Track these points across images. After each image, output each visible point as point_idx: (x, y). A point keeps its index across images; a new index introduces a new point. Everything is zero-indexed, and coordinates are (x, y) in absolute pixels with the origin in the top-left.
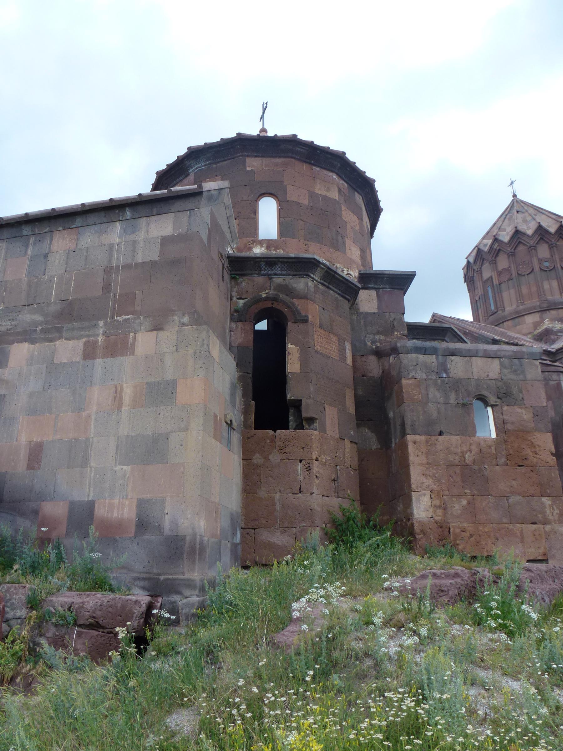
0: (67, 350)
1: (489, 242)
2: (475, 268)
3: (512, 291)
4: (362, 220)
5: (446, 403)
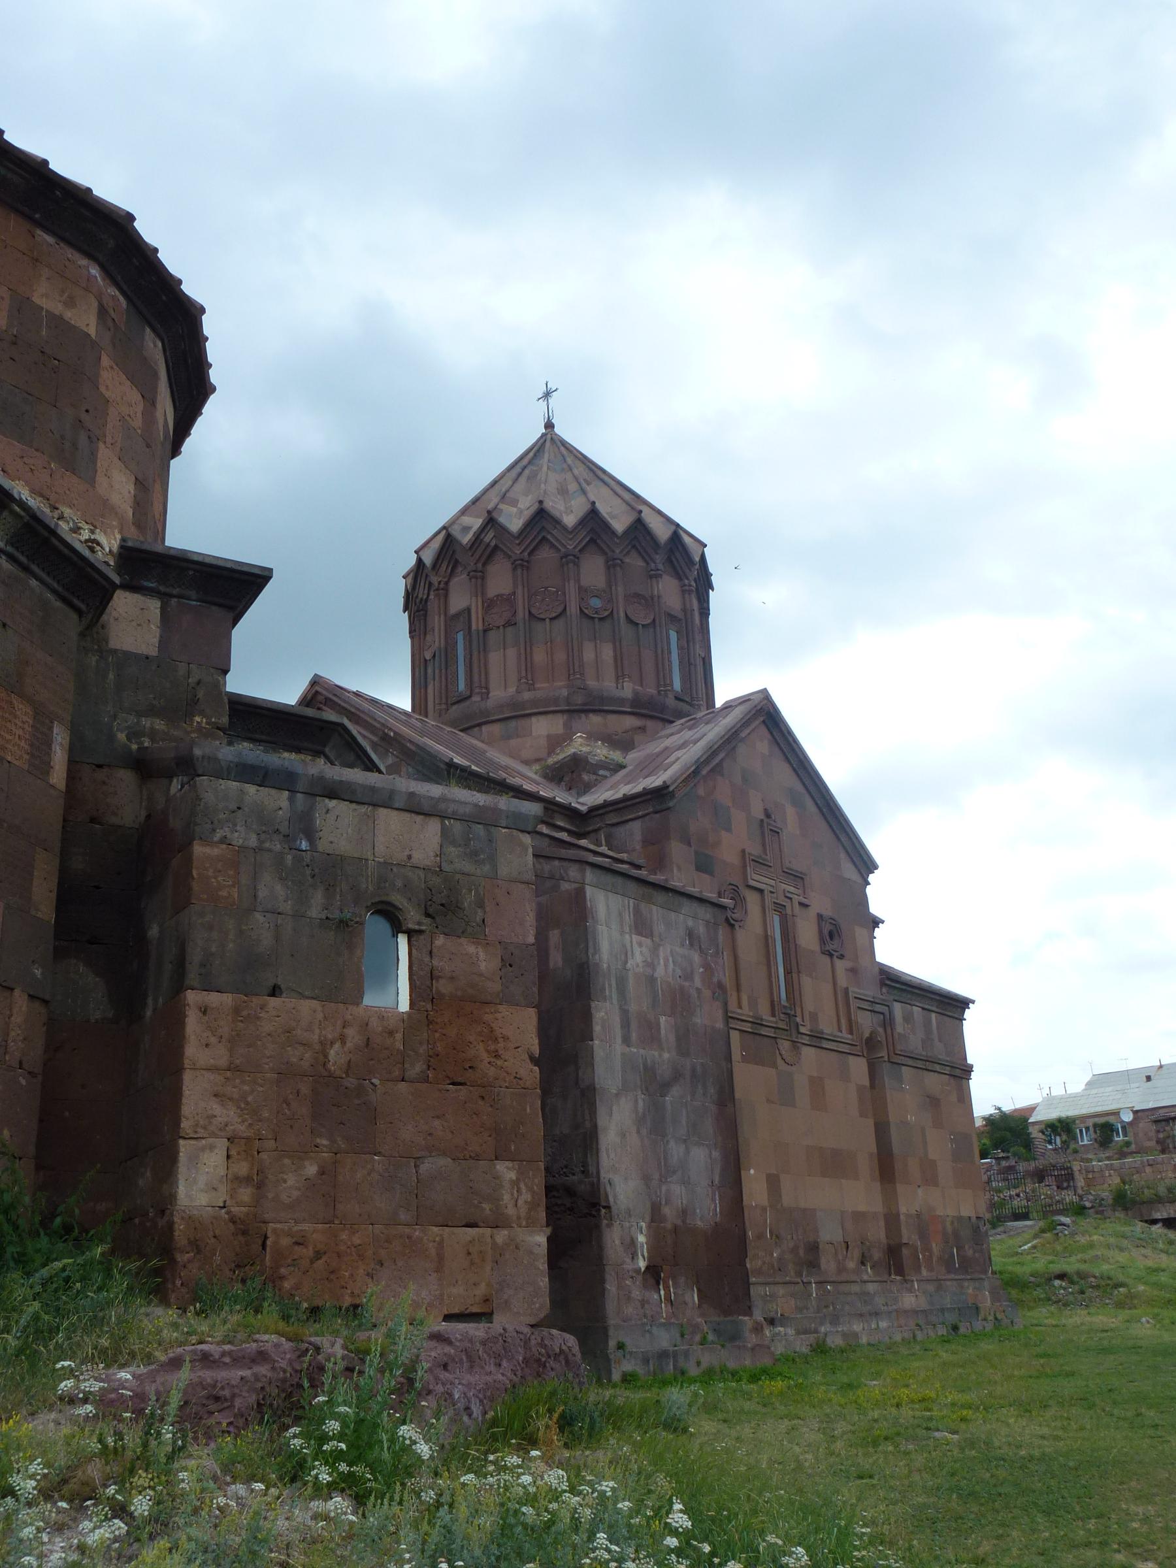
1: (476, 523)
2: (435, 580)
3: (511, 653)
4: (153, 404)
5: (298, 916)
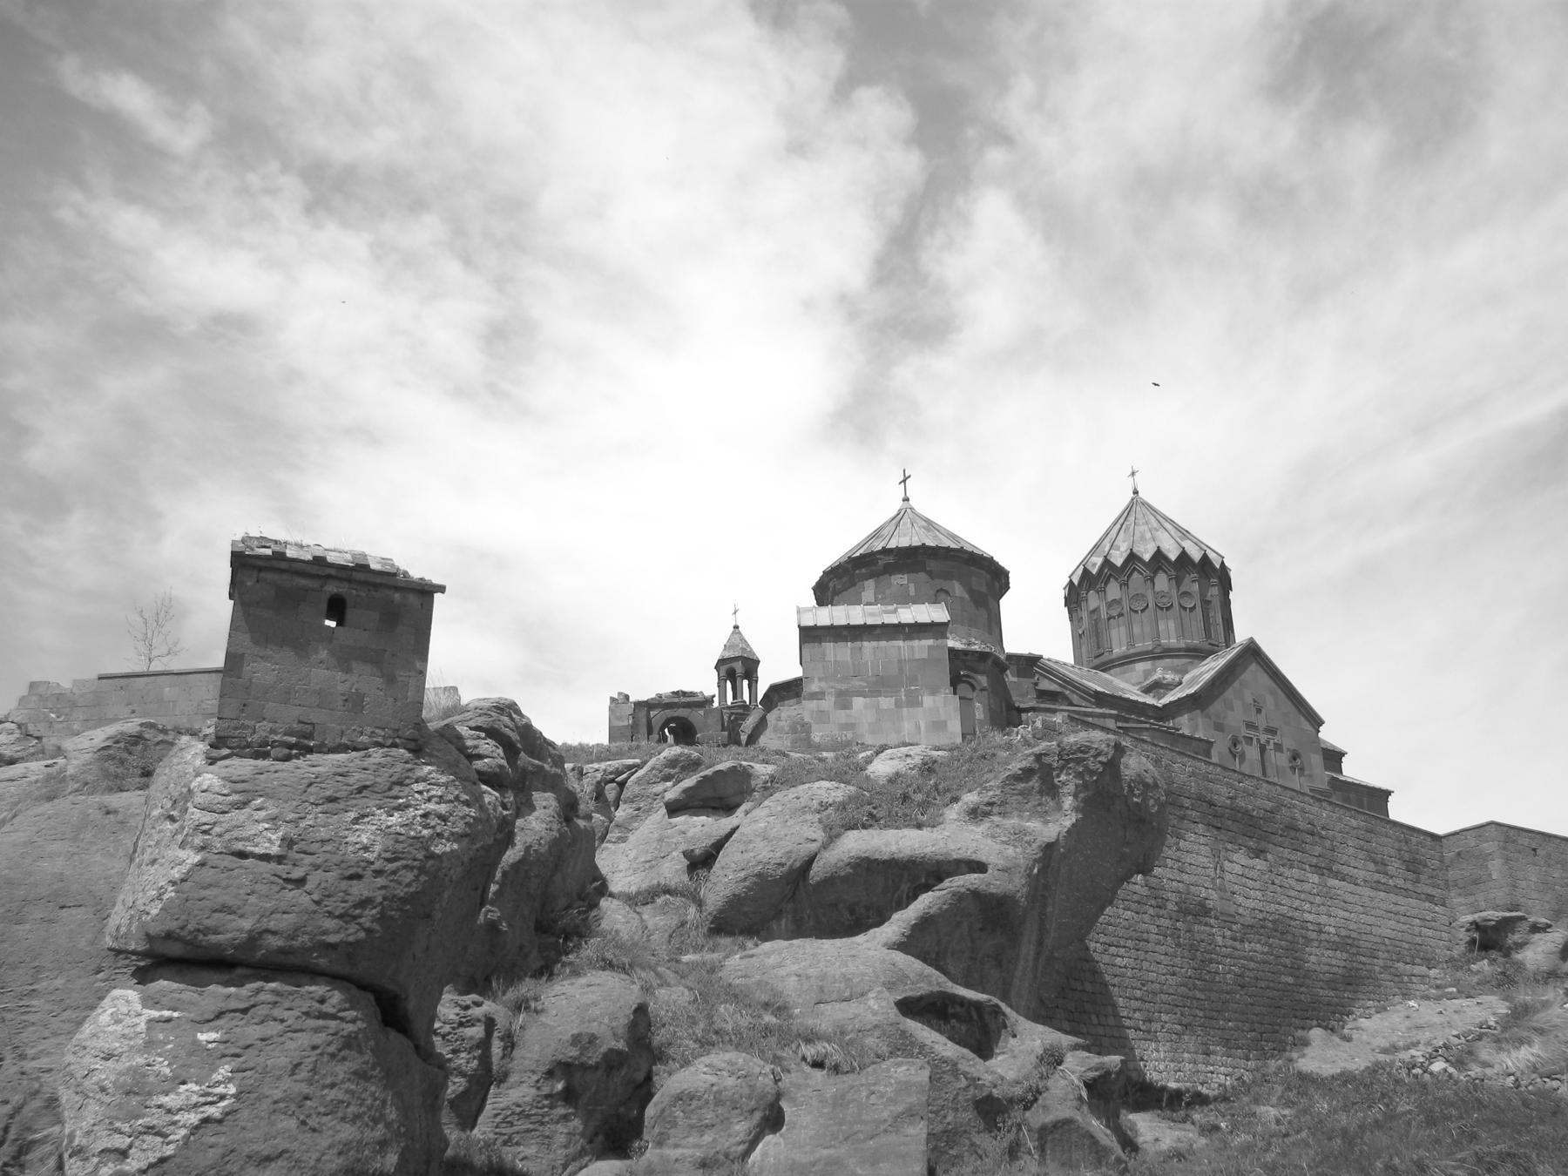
0: (886, 702)
1: (1099, 561)
3: (1123, 629)
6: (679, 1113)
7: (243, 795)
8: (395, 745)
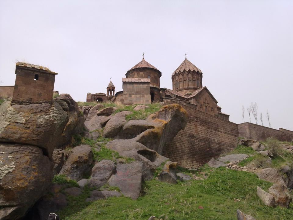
0: (138, 96)
1: (179, 71)
3: (182, 84)
6: (97, 171)
7: (18, 111)
8: (47, 103)
